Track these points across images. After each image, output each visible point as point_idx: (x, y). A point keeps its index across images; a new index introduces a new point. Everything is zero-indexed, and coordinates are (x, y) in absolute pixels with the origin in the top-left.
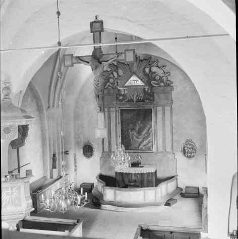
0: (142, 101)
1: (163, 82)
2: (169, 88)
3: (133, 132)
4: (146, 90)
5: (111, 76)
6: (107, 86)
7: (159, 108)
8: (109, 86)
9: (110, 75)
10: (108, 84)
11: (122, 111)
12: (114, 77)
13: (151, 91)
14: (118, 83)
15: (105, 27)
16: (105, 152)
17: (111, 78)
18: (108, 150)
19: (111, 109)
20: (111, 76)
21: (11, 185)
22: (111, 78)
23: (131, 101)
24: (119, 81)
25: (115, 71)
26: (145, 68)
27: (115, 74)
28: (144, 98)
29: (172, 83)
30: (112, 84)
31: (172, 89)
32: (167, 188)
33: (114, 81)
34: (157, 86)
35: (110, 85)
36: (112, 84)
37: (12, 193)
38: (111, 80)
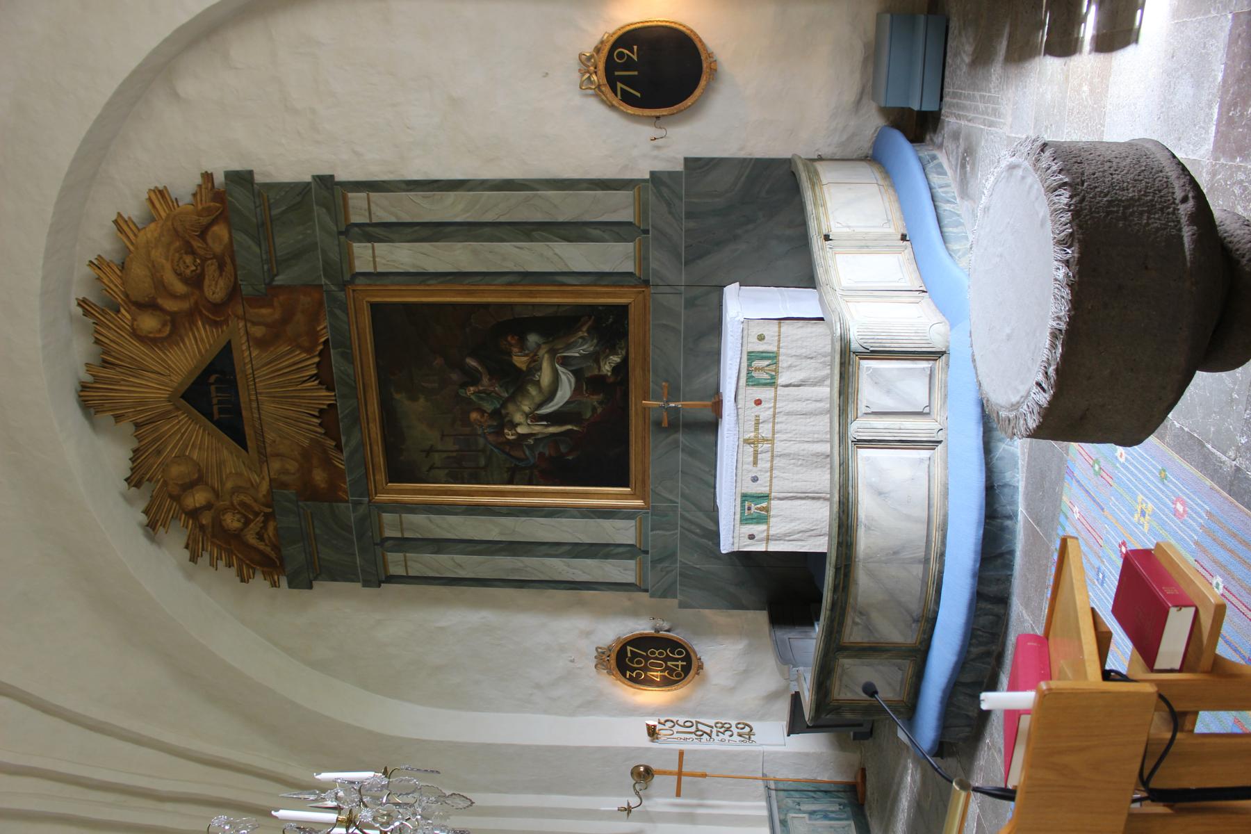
0: (324, 354)
1: (203, 233)
2: (240, 198)
3: (518, 418)
4: (258, 331)
5: (206, 519)
7: (365, 257)
8: (260, 537)
9: (202, 527)
10: (251, 539)
11: (400, 472)
12: (209, 506)
14: (236, 490)
16: (642, 574)
18: (632, 563)
19: (388, 533)
20: (206, 519)
22: (217, 523)
23: (327, 416)
27: (198, 498)
28: (309, 350)
29: (208, 177)
30: (247, 522)
31: (241, 179)
32: (865, 245)
33: (232, 507)
34: (229, 268)
35: (254, 527)
36: (247, 522)
38: (232, 522)
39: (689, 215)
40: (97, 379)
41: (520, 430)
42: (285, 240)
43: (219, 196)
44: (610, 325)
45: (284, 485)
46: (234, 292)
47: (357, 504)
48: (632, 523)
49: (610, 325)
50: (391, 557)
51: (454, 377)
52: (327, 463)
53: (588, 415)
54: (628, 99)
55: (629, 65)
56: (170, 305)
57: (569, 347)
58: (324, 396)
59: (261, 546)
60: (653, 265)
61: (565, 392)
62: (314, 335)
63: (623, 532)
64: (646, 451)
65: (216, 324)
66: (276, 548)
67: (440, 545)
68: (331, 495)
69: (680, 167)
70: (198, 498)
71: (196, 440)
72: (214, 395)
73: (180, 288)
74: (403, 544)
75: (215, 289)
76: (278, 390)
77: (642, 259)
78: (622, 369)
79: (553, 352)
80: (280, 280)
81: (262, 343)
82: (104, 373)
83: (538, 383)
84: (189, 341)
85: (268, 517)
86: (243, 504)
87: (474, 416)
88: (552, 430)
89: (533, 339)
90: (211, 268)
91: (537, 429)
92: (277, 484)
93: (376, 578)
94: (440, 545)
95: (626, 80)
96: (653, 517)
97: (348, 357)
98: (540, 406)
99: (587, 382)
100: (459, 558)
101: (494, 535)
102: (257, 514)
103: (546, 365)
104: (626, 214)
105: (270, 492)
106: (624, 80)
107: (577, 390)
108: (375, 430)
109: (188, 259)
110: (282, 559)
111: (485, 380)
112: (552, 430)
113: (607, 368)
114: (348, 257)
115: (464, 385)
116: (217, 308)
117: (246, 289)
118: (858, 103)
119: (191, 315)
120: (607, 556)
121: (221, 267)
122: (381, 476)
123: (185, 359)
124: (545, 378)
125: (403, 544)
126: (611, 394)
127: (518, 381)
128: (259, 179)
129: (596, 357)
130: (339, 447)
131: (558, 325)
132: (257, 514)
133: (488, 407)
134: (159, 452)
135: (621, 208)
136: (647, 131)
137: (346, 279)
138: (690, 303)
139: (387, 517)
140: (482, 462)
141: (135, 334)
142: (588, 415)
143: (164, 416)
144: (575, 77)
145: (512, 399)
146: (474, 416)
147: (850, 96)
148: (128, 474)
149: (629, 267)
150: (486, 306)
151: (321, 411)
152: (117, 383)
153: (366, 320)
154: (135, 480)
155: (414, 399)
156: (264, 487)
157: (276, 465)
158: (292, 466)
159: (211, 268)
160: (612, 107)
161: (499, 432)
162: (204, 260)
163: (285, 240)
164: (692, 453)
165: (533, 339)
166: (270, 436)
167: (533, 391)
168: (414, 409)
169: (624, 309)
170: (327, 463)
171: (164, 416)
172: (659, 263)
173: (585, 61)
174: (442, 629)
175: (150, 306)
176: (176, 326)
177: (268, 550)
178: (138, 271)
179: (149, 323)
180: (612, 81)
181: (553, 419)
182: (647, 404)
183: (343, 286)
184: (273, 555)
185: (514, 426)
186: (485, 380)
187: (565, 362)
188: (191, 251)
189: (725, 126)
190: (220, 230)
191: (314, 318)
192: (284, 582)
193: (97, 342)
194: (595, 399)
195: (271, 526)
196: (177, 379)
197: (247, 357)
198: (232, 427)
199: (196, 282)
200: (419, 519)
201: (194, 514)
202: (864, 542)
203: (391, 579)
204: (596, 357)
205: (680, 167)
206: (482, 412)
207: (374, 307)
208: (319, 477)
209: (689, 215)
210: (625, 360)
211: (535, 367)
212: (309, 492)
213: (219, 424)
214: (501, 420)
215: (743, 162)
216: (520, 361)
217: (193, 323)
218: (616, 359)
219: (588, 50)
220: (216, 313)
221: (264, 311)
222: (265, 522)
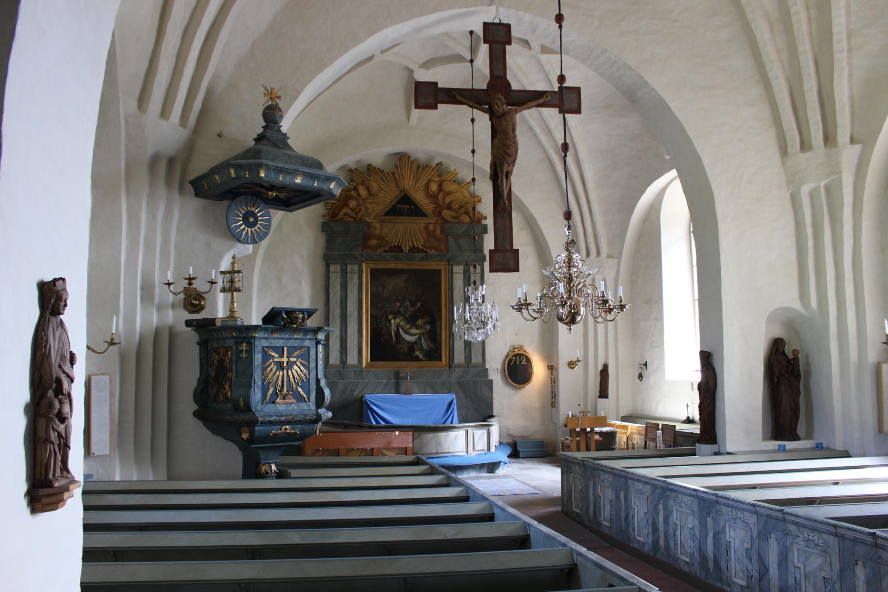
1: (467, 213)
3: (398, 320)
4: (431, 227)
5: (353, 193)
6: (340, 216)
7: (459, 270)
8: (346, 214)
9: (349, 191)
10: (344, 210)
11: (375, 274)
12: (359, 195)
13: (443, 230)
14: (367, 208)
15: (513, 34)
16: (333, 366)
17: (352, 198)
18: (338, 362)
19: (349, 267)
20: (353, 193)
21: (292, 343)
22: (352, 198)
23: (399, 249)
24: (369, 205)
25: (363, 183)
26: (430, 181)
27: (363, 192)
28: (424, 245)
30: (351, 209)
33: (359, 205)
34: (454, 221)
36: (352, 210)
37: (290, 365)
38: (352, 204)
39: (474, 382)
40: (412, 162)
41: (393, 321)
42: (464, 242)
43: (479, 221)
44: (434, 355)
45: (369, 228)
46: (445, 221)
47: (362, 255)
48: (356, 362)
49: (434, 355)
50: (338, 267)
51: (413, 298)
52: (379, 246)
53: (399, 346)
54: (510, 361)
55: (521, 361)
56: (440, 196)
57: (425, 340)
58: (406, 249)
59: (341, 214)
60: (457, 370)
61: (408, 338)
62: (430, 248)
63: (352, 359)
64: (386, 368)
65: (434, 212)
66: (341, 220)
67: (344, 287)
68: (365, 246)
69: (490, 378)
70: (363, 192)
71: (387, 196)
72: (405, 206)
73: (447, 201)
74: (344, 273)
75: (446, 214)
76: (408, 232)
77: (459, 366)
78: (417, 359)
79: (423, 334)
80: (450, 238)
81: (426, 228)
82: (415, 166)
83: (411, 328)
84: (427, 201)
85: (355, 219)
86: (360, 210)
87: (398, 304)
88: (393, 333)
89: (428, 327)
90: (454, 214)
91: (393, 327)
92: (369, 225)
93: (328, 259)
94: (344, 287)
95: (516, 360)
96: (359, 371)
97: (422, 259)
98: (402, 328)
99: (412, 346)
100: (339, 294)
101: (349, 309)
102: (356, 214)
103: (419, 331)
104: (474, 361)
105: (366, 222)
106: (516, 360)
107: (409, 342)
108: (392, 266)
109: (457, 206)
110: (336, 221)
111: (412, 309)
112: (393, 333)
113: (417, 353)
114: (458, 264)
115: (410, 301)
116: (440, 213)
117: (447, 225)
118: (510, 435)
119: (436, 203)
120: (341, 353)
121: (454, 218)
122: (372, 266)
123: (419, 197)
124: (413, 331)
125: (344, 273)
126: (408, 354)
127: (412, 321)
128: (485, 235)
129: (421, 349)
130: (385, 251)
131: (434, 336)
132: (356, 214)
133: (402, 310)
134: (383, 180)
135: (476, 359)
136: (499, 366)
137: (451, 262)
138: (443, 383)
139: (356, 267)
140: (379, 306)
141: (430, 181)
142: (399, 346)
143: (397, 185)
144: (516, 344)
145: (405, 318)
146: (398, 304)
147: (513, 432)
148: (373, 165)
149: (456, 361)
150: (440, 310)
151: (400, 247)
152: (411, 170)
153: (434, 267)
154: (370, 167)
155: (405, 282)
156: (368, 220)
157: (378, 226)
158: (377, 232)
159: (454, 214)
160: (507, 356)
161: (392, 313)
162: (457, 212)
163: (464, 242)
164: (386, 385)
165: (428, 327)
166: (389, 225)
167: (408, 326)
168: (400, 281)
169: (440, 359)
170: (379, 246)
171: (397, 185)
172: (458, 372)
173: (521, 347)
174: (300, 283)
175: (440, 189)
176: (433, 197)
177: (340, 216)
178: (451, 187)
179: (434, 187)
180: (515, 356)
181: (397, 333)
182: (407, 368)
183: (448, 261)
184: (338, 218)
185: (395, 319)
186: (412, 309)
187: (420, 338)
188: (460, 208)
189: (503, 394)
190: (466, 219)
191: (436, 249)
192: (322, 220)
193: (427, 166)
194: (405, 349)
195: (351, 220)
196: (412, 193)
197: (422, 222)
198: (394, 211)
199: (449, 207)
200: (356, 279)
201: (356, 189)
202: (442, 434)
203: (328, 266)
204: (421, 349)
205: (490, 378)
206: (400, 307)
207: (440, 271)
208: (373, 242)
209: (474, 382)
210: (421, 360)
211: (417, 327)
212: (367, 237)
213: (395, 206)
214: (396, 314)
215: (492, 399)
216: (420, 322)
217: (434, 203)
218: (421, 357)
219: (526, 348)
220: (438, 213)
221: (439, 231)
222: (352, 217)
